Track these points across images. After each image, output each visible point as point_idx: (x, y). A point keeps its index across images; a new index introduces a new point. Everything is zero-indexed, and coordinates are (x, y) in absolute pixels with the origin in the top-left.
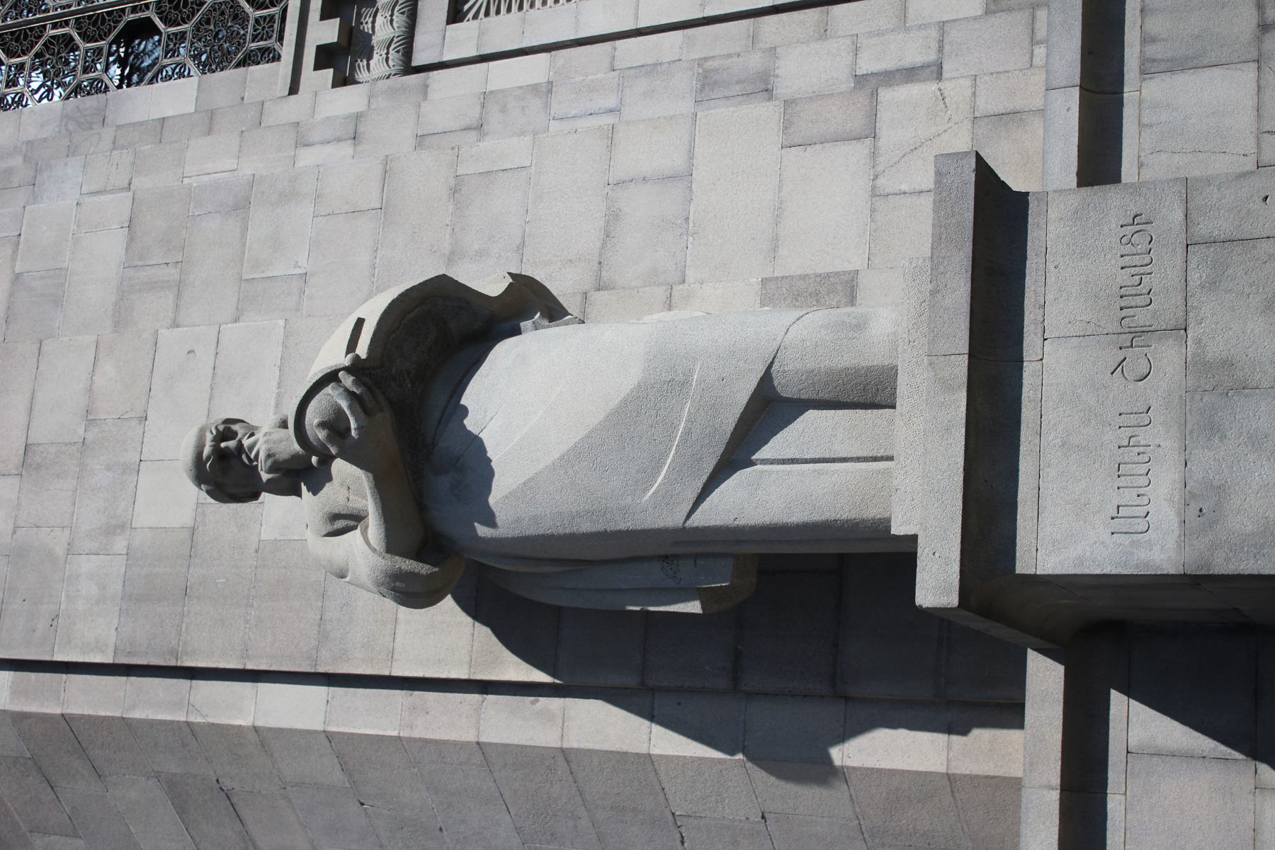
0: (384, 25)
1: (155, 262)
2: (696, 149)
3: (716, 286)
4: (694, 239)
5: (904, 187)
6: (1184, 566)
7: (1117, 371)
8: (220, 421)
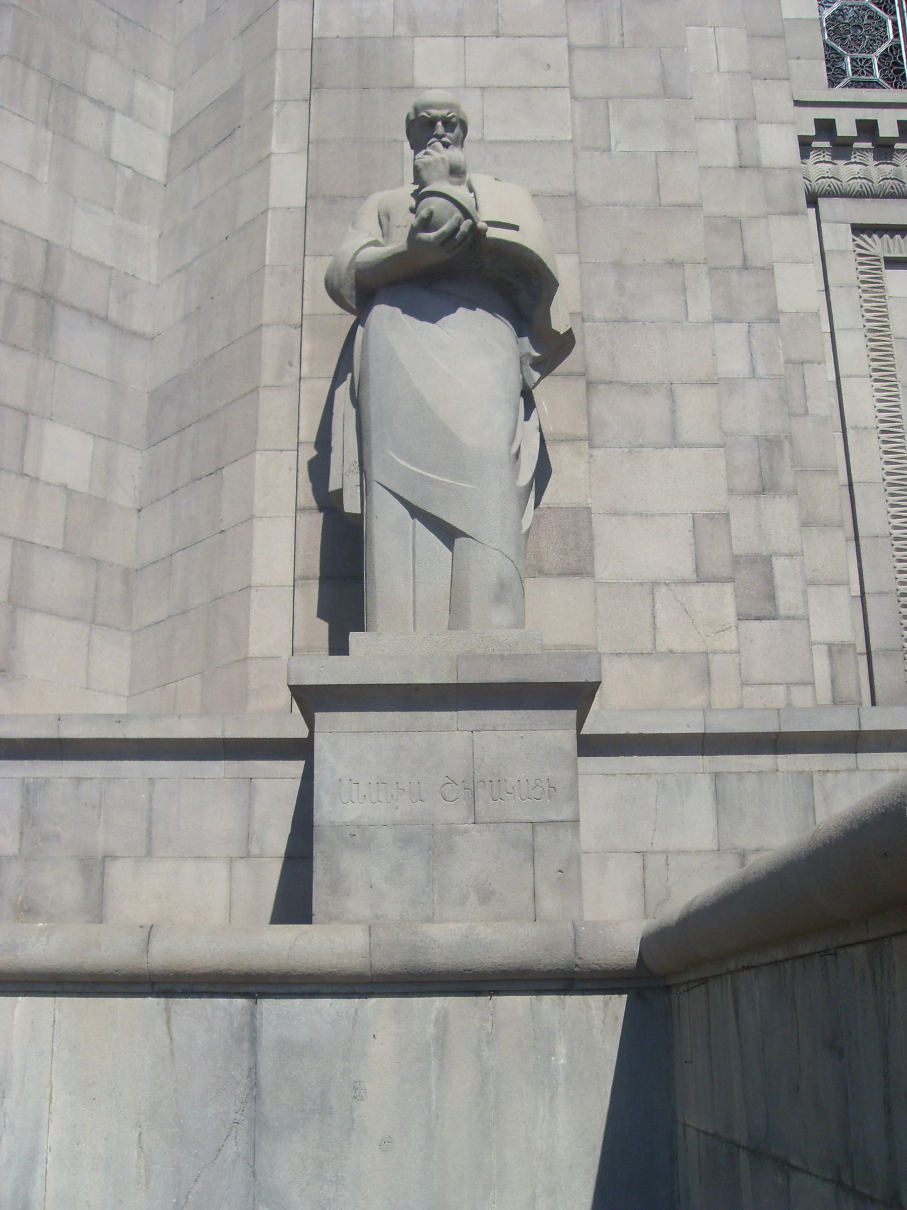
0: (852, 172)
1: (624, 24)
2: (695, 449)
3: (586, 473)
4: (627, 452)
5: (658, 606)
6: (318, 826)
7: (449, 780)
8: (461, 117)
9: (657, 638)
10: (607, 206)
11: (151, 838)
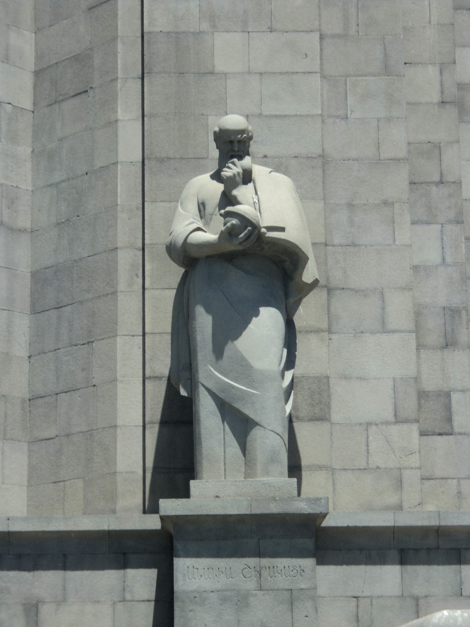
1: (359, 16)
4: (352, 337)
5: (371, 438)
9: (369, 459)
10: (344, 160)
11: (65, 590)
